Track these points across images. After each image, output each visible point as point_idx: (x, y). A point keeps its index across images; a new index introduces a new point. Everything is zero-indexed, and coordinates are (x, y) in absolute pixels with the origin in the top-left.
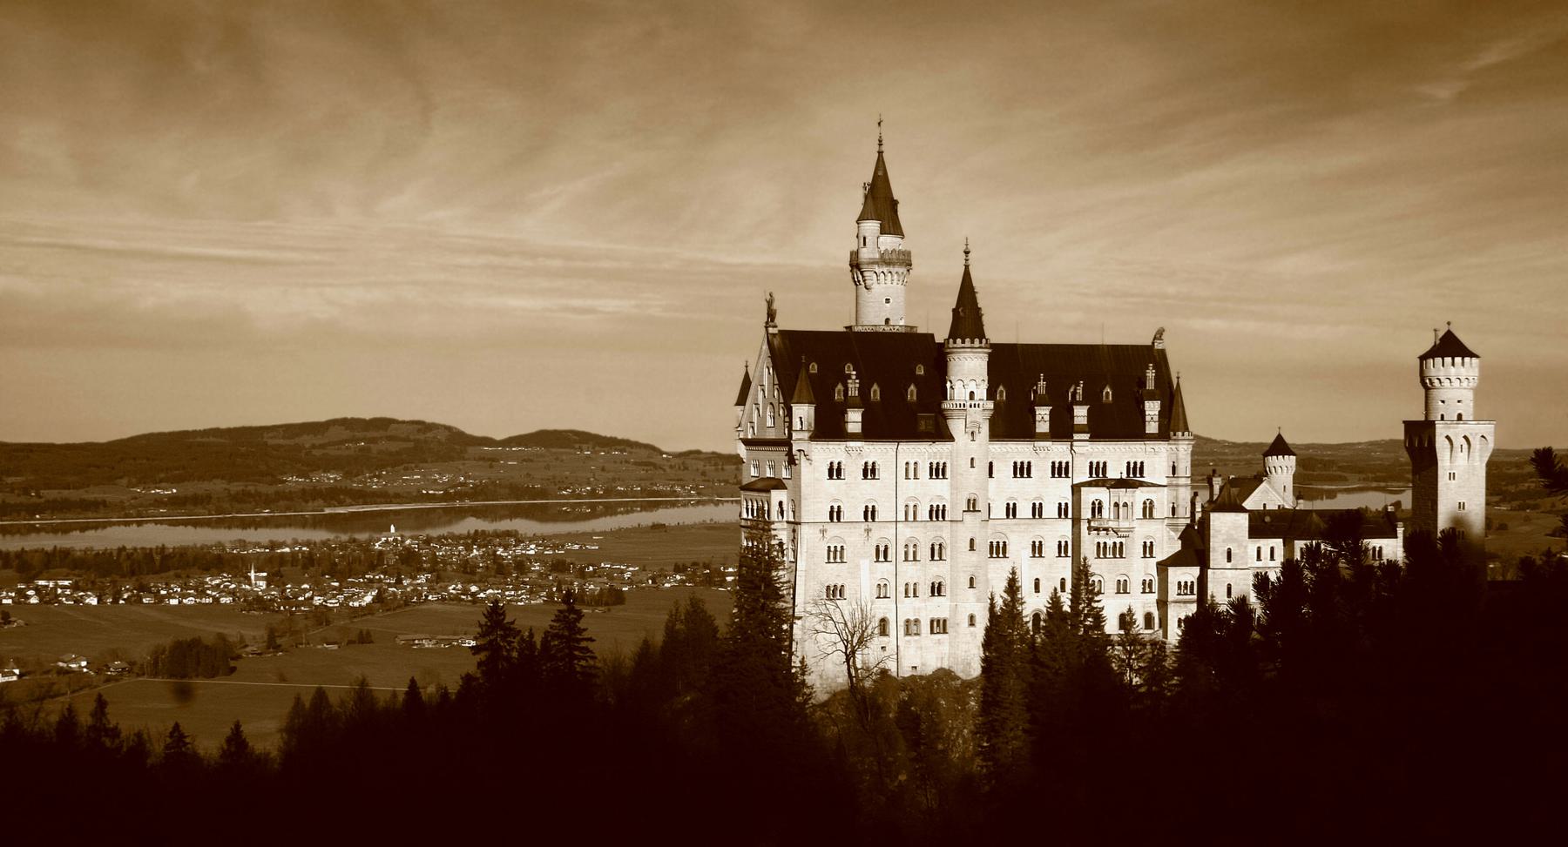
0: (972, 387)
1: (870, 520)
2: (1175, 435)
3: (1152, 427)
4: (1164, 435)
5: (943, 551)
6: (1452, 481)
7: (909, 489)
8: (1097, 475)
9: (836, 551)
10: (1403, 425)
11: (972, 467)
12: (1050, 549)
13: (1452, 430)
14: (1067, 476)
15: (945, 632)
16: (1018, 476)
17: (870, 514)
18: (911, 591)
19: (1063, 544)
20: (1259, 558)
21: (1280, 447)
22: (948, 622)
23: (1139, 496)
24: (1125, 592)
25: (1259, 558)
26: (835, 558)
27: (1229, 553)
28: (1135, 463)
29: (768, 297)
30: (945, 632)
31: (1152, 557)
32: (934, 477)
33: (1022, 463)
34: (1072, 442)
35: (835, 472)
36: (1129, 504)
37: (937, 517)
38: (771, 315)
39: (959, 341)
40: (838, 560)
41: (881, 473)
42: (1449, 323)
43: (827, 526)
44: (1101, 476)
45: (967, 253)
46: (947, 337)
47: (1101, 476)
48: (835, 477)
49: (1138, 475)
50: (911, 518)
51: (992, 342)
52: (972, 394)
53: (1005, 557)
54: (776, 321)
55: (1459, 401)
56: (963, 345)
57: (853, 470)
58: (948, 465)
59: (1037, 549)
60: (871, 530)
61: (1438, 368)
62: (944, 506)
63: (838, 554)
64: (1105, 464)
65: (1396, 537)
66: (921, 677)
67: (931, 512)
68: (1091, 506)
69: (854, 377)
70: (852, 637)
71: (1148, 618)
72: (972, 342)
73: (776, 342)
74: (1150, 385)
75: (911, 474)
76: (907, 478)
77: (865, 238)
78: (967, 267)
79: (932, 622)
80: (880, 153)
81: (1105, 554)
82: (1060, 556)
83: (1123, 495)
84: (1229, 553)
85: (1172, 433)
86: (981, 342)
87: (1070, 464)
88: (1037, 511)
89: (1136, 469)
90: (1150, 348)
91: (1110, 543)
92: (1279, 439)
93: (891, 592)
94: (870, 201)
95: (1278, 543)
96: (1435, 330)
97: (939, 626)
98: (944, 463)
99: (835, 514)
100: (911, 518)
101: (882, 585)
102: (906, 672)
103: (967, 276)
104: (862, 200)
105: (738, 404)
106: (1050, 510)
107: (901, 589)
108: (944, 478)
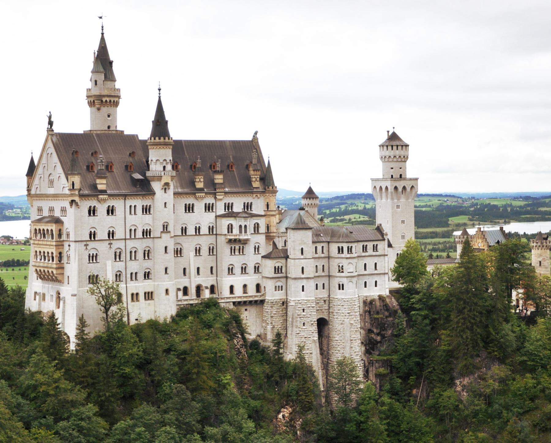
0: (164, 164)
1: (111, 238)
2: (268, 188)
3: (256, 184)
5: (150, 254)
6: (399, 210)
7: (132, 220)
8: (228, 209)
9: (93, 257)
10: (371, 181)
12: (205, 251)
13: (398, 183)
14: (212, 211)
15: (152, 299)
16: (187, 211)
17: (111, 234)
18: (134, 276)
19: (211, 248)
20: (316, 253)
21: (310, 194)
22: (153, 294)
23: (250, 223)
24: (245, 273)
25: (316, 253)
26: (93, 260)
27: (302, 249)
28: (248, 203)
29: (49, 114)
30: (152, 299)
31: (259, 254)
32: (145, 213)
33: (189, 204)
34: (215, 194)
35: (92, 212)
36: (248, 227)
37: (147, 236)
38: (51, 123)
39: (157, 138)
40: (95, 261)
42: (394, 128)
43: (88, 243)
44: (230, 210)
45: (159, 90)
46: (149, 136)
47: (230, 210)
48: (92, 215)
49: (249, 210)
50: (133, 237)
51: (174, 139)
52: (164, 167)
53: (181, 256)
54: (53, 128)
55: (400, 168)
56: (159, 141)
57: (102, 209)
58: (152, 206)
59: (198, 251)
60: (112, 244)
61: (389, 152)
62: (150, 229)
63: (94, 258)
64: (232, 204)
65: (384, 240)
66: (143, 324)
67: (143, 233)
68: (227, 227)
71: (258, 287)
72: (165, 139)
73: (55, 139)
74: (254, 161)
77: (96, 81)
78: (160, 97)
79: (145, 293)
80: (103, 34)
81: (234, 253)
82: (210, 255)
83: (243, 223)
84: (302, 249)
85: (267, 187)
86: (169, 139)
87: (214, 205)
88: (198, 230)
89: (248, 206)
90: (252, 141)
91: (237, 247)
93: (123, 278)
95: (325, 245)
96: (388, 132)
97: (149, 296)
98: (150, 206)
99: (93, 235)
100: (133, 237)
101: (118, 274)
102: (133, 322)
104: (92, 59)
106: (204, 230)
107: (129, 276)
108: (150, 214)
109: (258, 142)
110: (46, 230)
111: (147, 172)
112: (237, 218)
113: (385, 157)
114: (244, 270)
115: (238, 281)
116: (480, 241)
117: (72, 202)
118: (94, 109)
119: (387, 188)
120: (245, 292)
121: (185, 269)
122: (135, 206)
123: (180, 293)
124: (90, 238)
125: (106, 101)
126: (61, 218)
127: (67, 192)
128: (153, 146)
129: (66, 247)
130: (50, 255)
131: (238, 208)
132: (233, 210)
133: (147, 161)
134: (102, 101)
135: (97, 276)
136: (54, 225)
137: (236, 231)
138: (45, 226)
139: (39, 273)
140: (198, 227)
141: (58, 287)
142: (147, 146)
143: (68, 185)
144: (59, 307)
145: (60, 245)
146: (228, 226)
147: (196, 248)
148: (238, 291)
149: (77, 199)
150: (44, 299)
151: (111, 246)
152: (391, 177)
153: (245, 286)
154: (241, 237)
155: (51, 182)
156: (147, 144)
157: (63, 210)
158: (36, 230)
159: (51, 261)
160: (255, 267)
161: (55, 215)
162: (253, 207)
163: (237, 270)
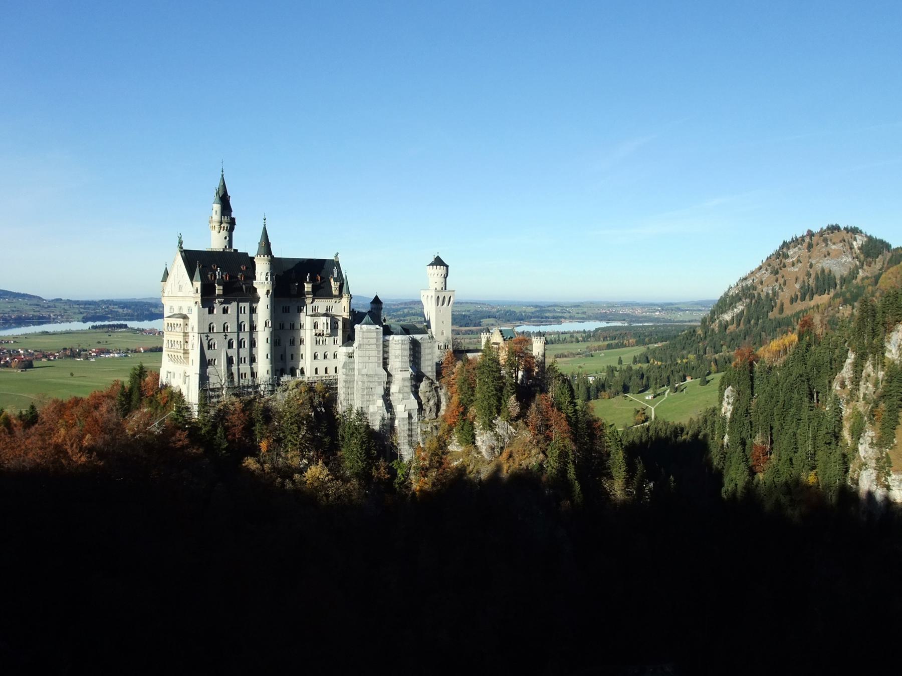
3: (335, 292)
4: (340, 296)
8: (315, 311)
11: (268, 308)
17: (225, 328)
21: (377, 301)
28: (330, 307)
29: (180, 236)
38: (181, 243)
40: (213, 348)
41: (229, 312)
43: (208, 334)
44: (316, 311)
45: (265, 219)
50: (243, 331)
54: (182, 246)
69: (219, 271)
70: (221, 381)
73: (183, 254)
75: (243, 312)
76: (241, 313)
77: (216, 211)
78: (265, 225)
81: (319, 343)
85: (344, 295)
89: (329, 309)
90: (333, 260)
92: (377, 297)
94: (218, 195)
99: (211, 329)
100: (243, 331)
103: (265, 229)
105: (162, 281)
109: (338, 262)
110: (176, 324)
111: (254, 281)
112: (321, 317)
113: (431, 274)
114: (325, 357)
115: (321, 364)
116: (497, 336)
117: (196, 302)
118: (214, 233)
119: (432, 296)
120: (326, 373)
121: (282, 355)
122: (244, 307)
123: (278, 373)
124: (210, 330)
125: (224, 227)
126: (188, 315)
127: (193, 295)
128: (258, 262)
129: (191, 338)
130: (179, 343)
131: (322, 310)
132: (319, 312)
133: (254, 273)
134: (221, 227)
135: (215, 360)
136: (182, 320)
137: (320, 327)
138: (175, 320)
139: (170, 357)
140: (292, 323)
141: (184, 367)
142: (255, 262)
143: (193, 290)
144: (185, 383)
145: (186, 334)
146: (315, 323)
147: (291, 340)
148: (321, 372)
149: (199, 300)
150: (174, 377)
151: (227, 337)
152: (435, 289)
153: (326, 369)
154: (325, 332)
155: (180, 289)
156: (254, 260)
157: (190, 310)
158: (168, 324)
159: (179, 348)
160: (334, 354)
161: (183, 313)
162: (333, 309)
163: (320, 356)
